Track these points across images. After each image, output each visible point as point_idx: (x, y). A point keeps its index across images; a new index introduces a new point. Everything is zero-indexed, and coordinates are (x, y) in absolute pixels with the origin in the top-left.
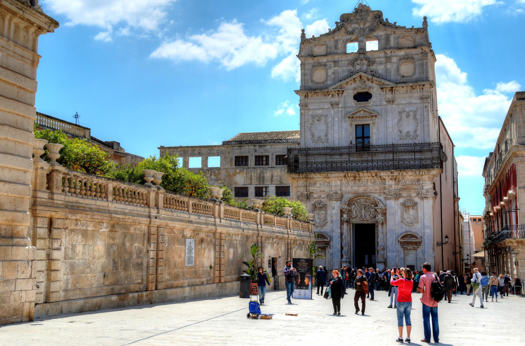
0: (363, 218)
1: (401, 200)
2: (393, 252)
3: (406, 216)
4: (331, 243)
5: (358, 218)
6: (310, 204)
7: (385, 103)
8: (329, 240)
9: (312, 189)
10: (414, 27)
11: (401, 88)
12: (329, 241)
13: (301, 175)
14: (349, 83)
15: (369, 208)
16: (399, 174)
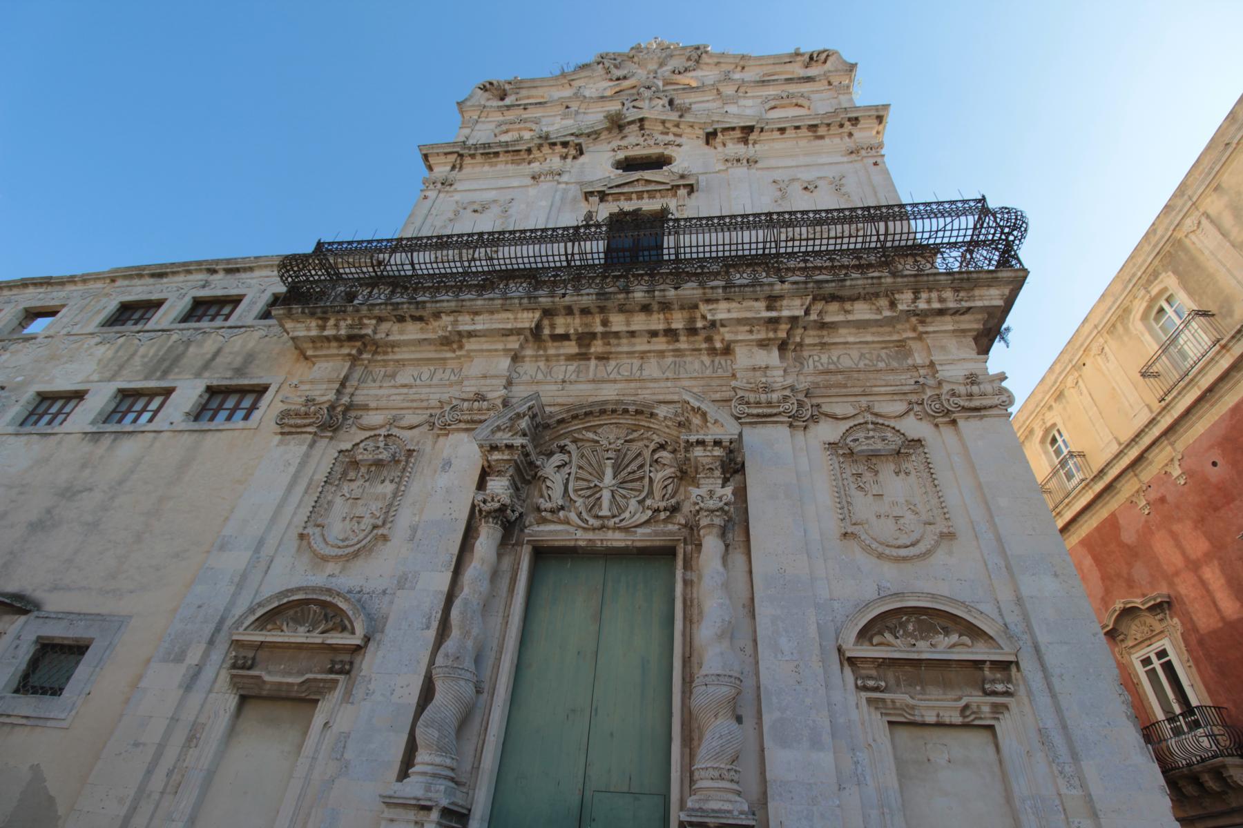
0: (605, 512)
1: (827, 431)
2: (816, 744)
3: (863, 506)
4: (369, 664)
5: (573, 516)
6: (326, 454)
7: (720, 166)
8: (356, 640)
9: (368, 393)
10: (802, 51)
11: (777, 134)
12: (358, 648)
13: (332, 322)
14: (603, 137)
15: (641, 466)
16: (807, 312)
